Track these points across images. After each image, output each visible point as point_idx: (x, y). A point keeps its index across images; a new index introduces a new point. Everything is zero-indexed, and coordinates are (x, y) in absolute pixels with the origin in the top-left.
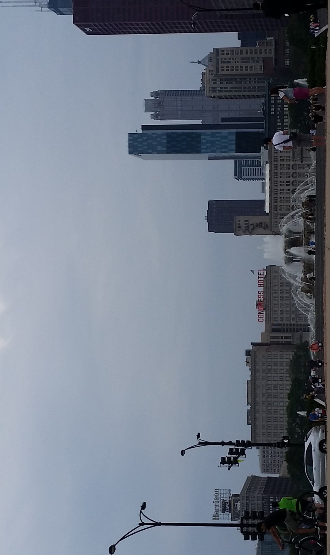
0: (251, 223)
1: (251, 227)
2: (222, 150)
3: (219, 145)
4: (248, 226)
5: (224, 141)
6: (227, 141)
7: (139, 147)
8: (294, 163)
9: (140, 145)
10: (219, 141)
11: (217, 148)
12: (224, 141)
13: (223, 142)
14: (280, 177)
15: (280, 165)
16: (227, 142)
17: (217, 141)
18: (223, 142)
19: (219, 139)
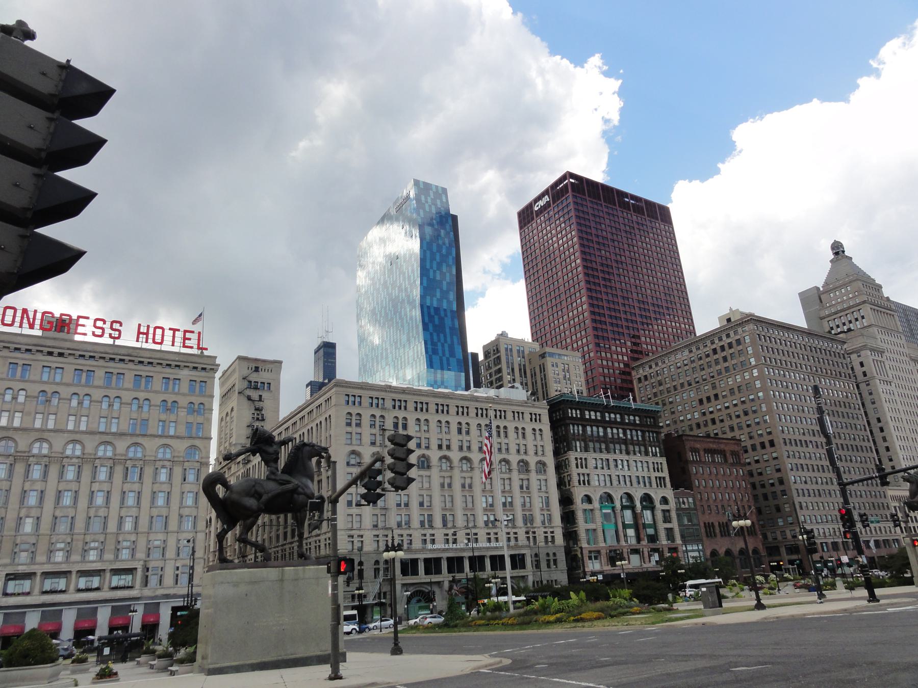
0: (265, 395)
1: (255, 395)
2: (429, 343)
3: (439, 340)
4: (256, 388)
5: (447, 348)
6: (447, 355)
7: (426, 198)
8: (514, 465)
9: (429, 200)
10: (446, 341)
11: (431, 334)
12: (447, 348)
13: (443, 346)
14: (479, 425)
15: (505, 427)
16: (444, 354)
17: (445, 336)
18: (443, 346)
19: (449, 339)
